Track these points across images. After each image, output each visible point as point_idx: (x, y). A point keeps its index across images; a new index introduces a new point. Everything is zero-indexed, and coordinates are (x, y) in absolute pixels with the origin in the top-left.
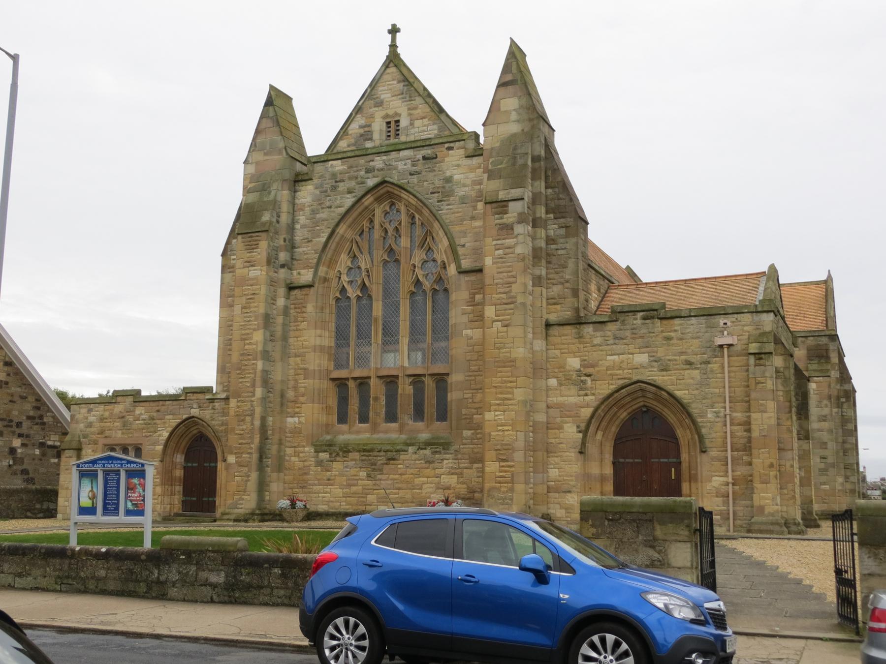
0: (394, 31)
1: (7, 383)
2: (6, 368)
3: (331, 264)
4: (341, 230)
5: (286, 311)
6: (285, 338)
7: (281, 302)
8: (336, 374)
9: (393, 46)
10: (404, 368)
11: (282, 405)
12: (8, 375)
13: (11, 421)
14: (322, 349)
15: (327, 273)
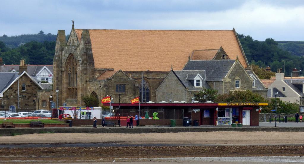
0: (73, 22)
1: (31, 86)
2: (31, 82)
3: (67, 67)
4: (67, 61)
5: (61, 76)
6: (61, 81)
7: (60, 74)
8: (69, 88)
9: (73, 26)
10: (75, 87)
11: (61, 93)
12: (31, 84)
13: (33, 94)
14: (66, 83)
15: (66, 69)
